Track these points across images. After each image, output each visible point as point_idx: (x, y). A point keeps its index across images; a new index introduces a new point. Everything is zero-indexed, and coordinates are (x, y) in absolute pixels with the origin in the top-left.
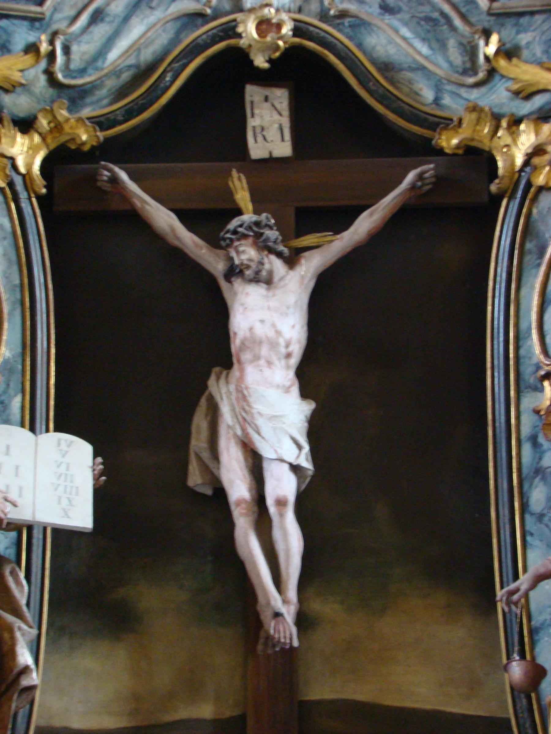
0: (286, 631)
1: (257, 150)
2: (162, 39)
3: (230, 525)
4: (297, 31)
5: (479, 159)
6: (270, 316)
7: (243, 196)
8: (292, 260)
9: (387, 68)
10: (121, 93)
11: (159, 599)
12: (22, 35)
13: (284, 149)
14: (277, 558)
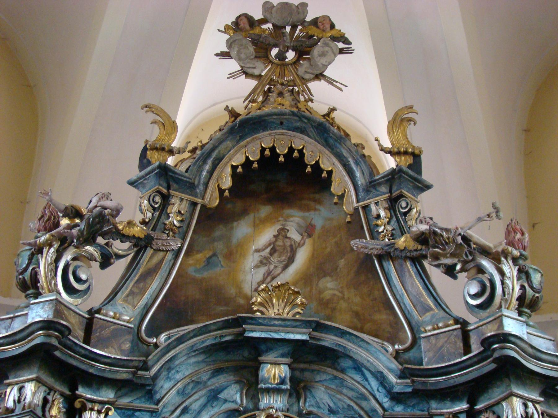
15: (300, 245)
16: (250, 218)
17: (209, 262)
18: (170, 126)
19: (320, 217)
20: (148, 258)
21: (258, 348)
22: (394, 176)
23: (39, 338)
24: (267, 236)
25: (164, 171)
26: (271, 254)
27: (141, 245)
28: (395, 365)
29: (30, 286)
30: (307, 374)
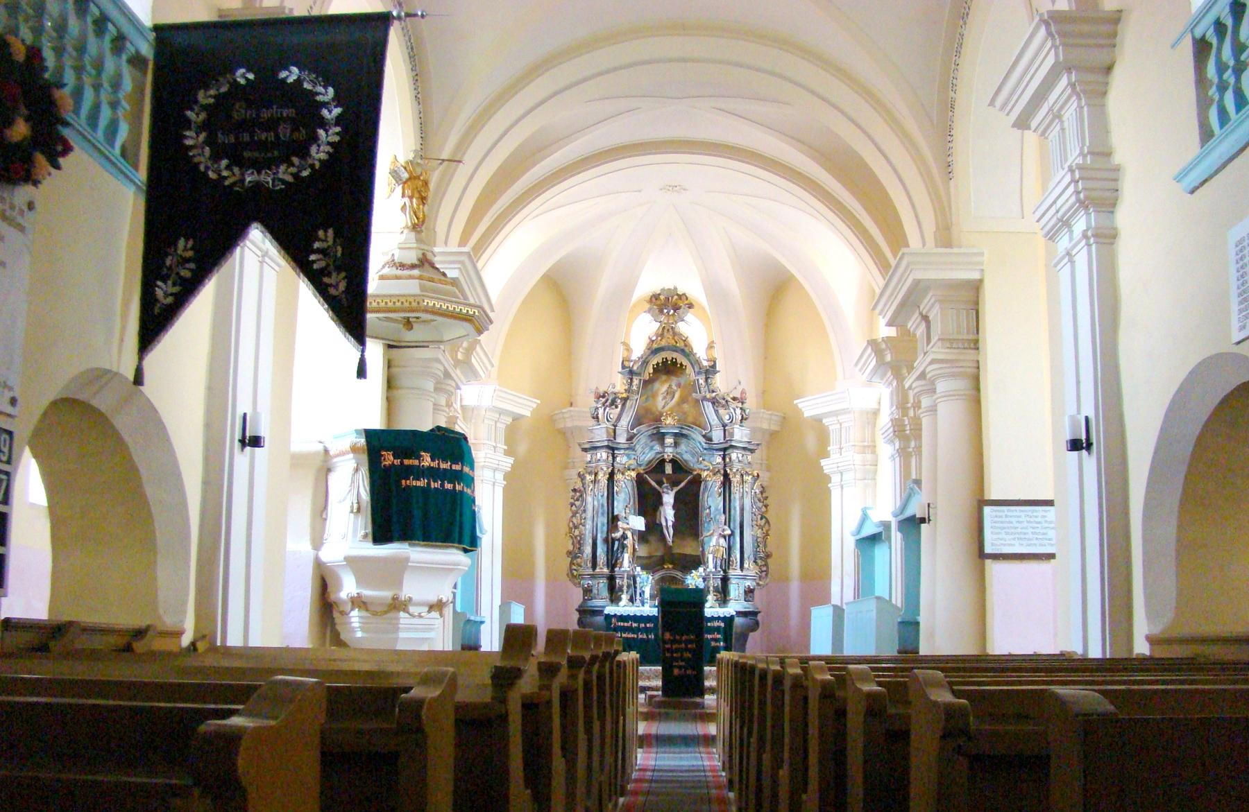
5: (700, 475)
6: (669, 499)
11: (652, 539)
14: (669, 534)
18: (628, 349)
19: (682, 380)
21: (664, 435)
22: (707, 372)
24: (664, 388)
25: (631, 372)
27: (625, 400)
29: (596, 418)
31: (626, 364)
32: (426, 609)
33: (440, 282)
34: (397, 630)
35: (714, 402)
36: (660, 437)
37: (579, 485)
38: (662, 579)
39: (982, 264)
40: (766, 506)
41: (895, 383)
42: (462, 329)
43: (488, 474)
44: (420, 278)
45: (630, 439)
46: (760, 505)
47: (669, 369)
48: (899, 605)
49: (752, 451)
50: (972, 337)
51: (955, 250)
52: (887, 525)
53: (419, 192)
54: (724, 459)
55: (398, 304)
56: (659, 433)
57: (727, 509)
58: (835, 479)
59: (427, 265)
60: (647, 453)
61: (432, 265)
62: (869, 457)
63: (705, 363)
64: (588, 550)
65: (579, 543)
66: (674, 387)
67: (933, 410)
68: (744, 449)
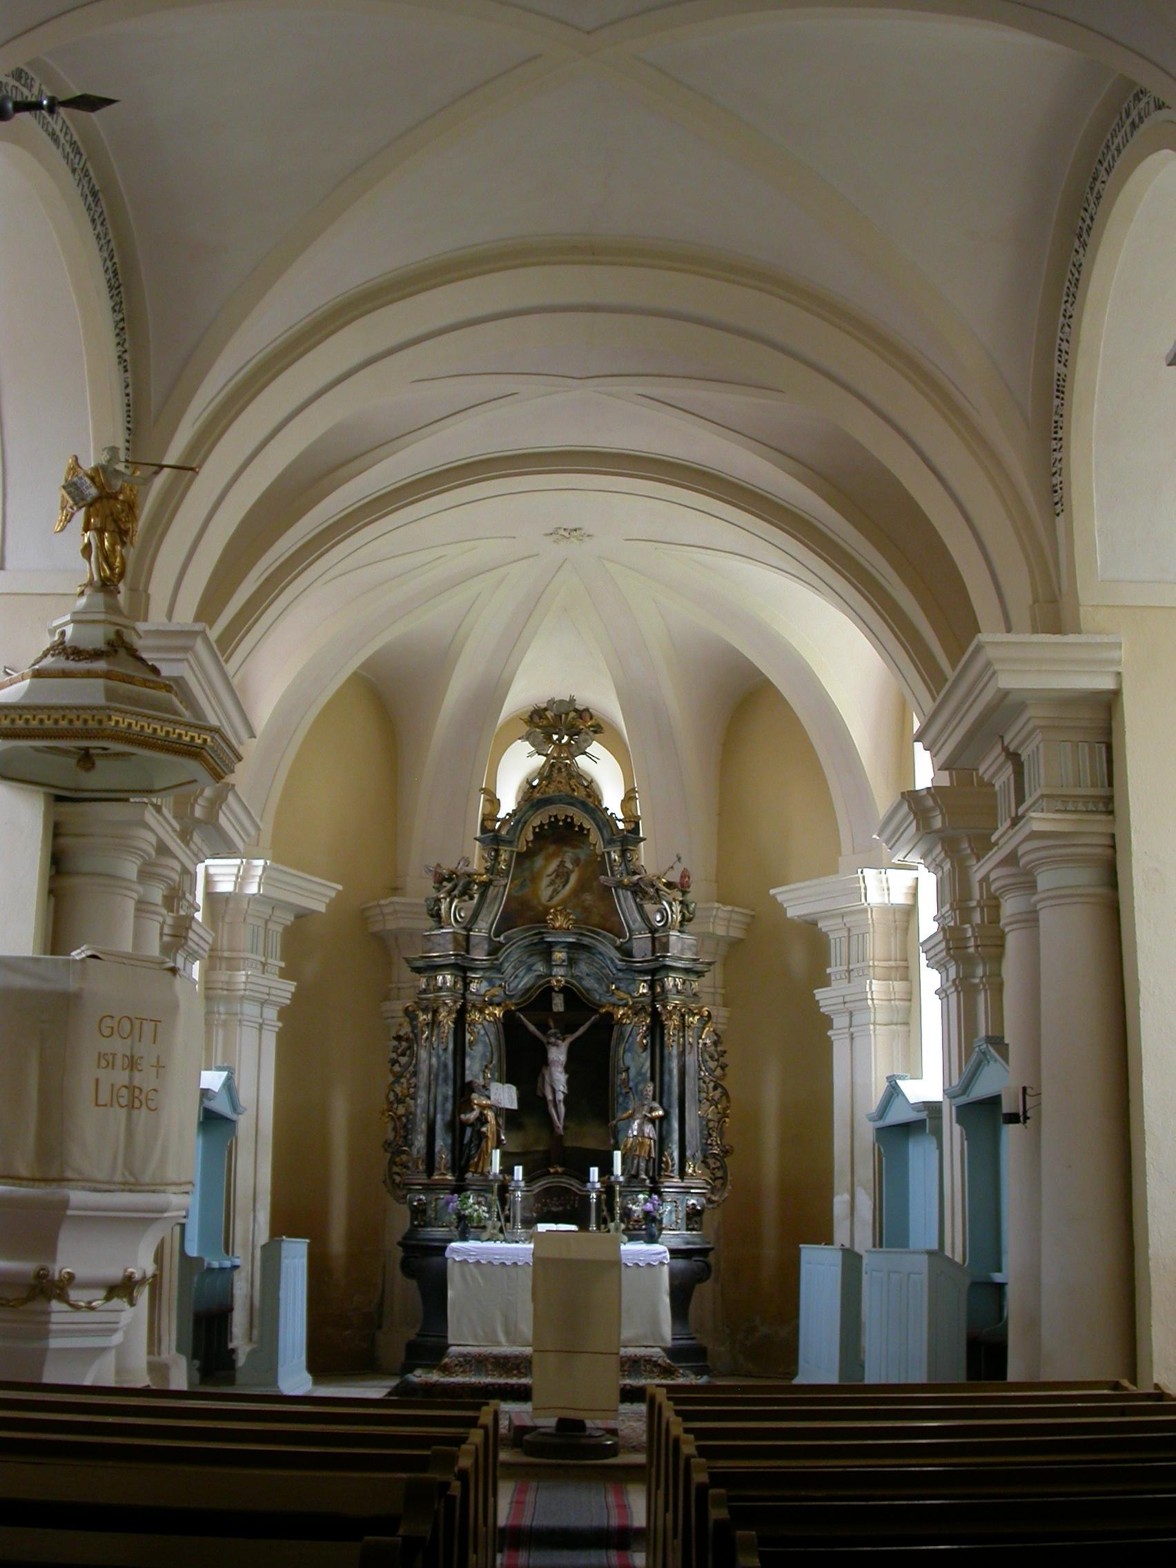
0: (561, 1131)
1: (555, 1009)
2: (532, 981)
3: (547, 1106)
4: (567, 982)
5: (610, 1015)
6: (558, 1054)
7: (551, 1024)
8: (563, 1040)
9: (587, 990)
10: (522, 996)
12: (498, 982)
13: (562, 1009)
14: (559, 1114)
15: (572, 871)
16: (543, 853)
17: (522, 885)
18: (494, 803)
20: (492, 891)
21: (550, 945)
23: (452, 960)
24: (553, 866)
26: (557, 876)
27: (485, 886)
28: (618, 955)
29: (436, 915)
30: (576, 956)
31: (489, 824)
32: (103, 1293)
33: (145, 683)
34: (45, 1334)
35: (638, 890)
36: (546, 951)
37: (406, 1030)
38: (547, 1191)
39: (1119, 662)
40: (723, 1067)
41: (947, 866)
42: (192, 768)
43: (251, 1010)
44: (107, 675)
45: (494, 950)
46: (712, 1064)
47: (561, 834)
48: (958, 1258)
49: (699, 974)
50: (1102, 791)
51: (1071, 638)
52: (932, 1108)
53: (116, 521)
54: (652, 987)
55: (64, 724)
56: (542, 941)
57: (658, 1072)
58: (840, 1022)
59: (122, 653)
60: (521, 978)
61: (133, 653)
62: (899, 986)
63: (621, 825)
64: (420, 1141)
65: (404, 1128)
66: (569, 865)
67: (1031, 919)
68: (687, 971)
